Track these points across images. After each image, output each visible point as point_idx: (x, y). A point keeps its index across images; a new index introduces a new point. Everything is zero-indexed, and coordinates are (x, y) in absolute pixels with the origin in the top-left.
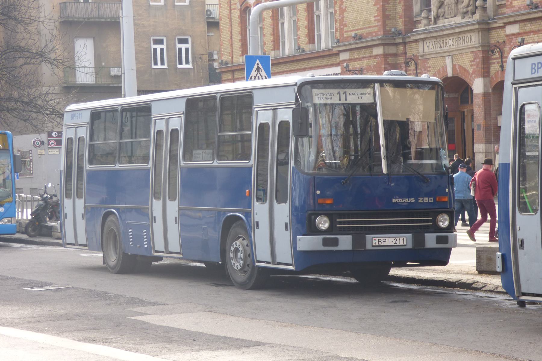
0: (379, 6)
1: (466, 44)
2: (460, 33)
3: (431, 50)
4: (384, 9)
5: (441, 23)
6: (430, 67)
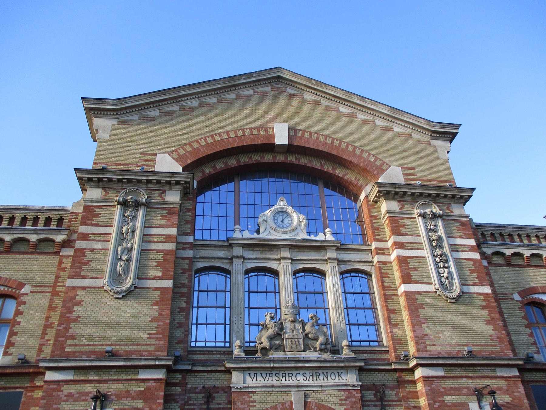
2: (320, 368)
6: (255, 402)
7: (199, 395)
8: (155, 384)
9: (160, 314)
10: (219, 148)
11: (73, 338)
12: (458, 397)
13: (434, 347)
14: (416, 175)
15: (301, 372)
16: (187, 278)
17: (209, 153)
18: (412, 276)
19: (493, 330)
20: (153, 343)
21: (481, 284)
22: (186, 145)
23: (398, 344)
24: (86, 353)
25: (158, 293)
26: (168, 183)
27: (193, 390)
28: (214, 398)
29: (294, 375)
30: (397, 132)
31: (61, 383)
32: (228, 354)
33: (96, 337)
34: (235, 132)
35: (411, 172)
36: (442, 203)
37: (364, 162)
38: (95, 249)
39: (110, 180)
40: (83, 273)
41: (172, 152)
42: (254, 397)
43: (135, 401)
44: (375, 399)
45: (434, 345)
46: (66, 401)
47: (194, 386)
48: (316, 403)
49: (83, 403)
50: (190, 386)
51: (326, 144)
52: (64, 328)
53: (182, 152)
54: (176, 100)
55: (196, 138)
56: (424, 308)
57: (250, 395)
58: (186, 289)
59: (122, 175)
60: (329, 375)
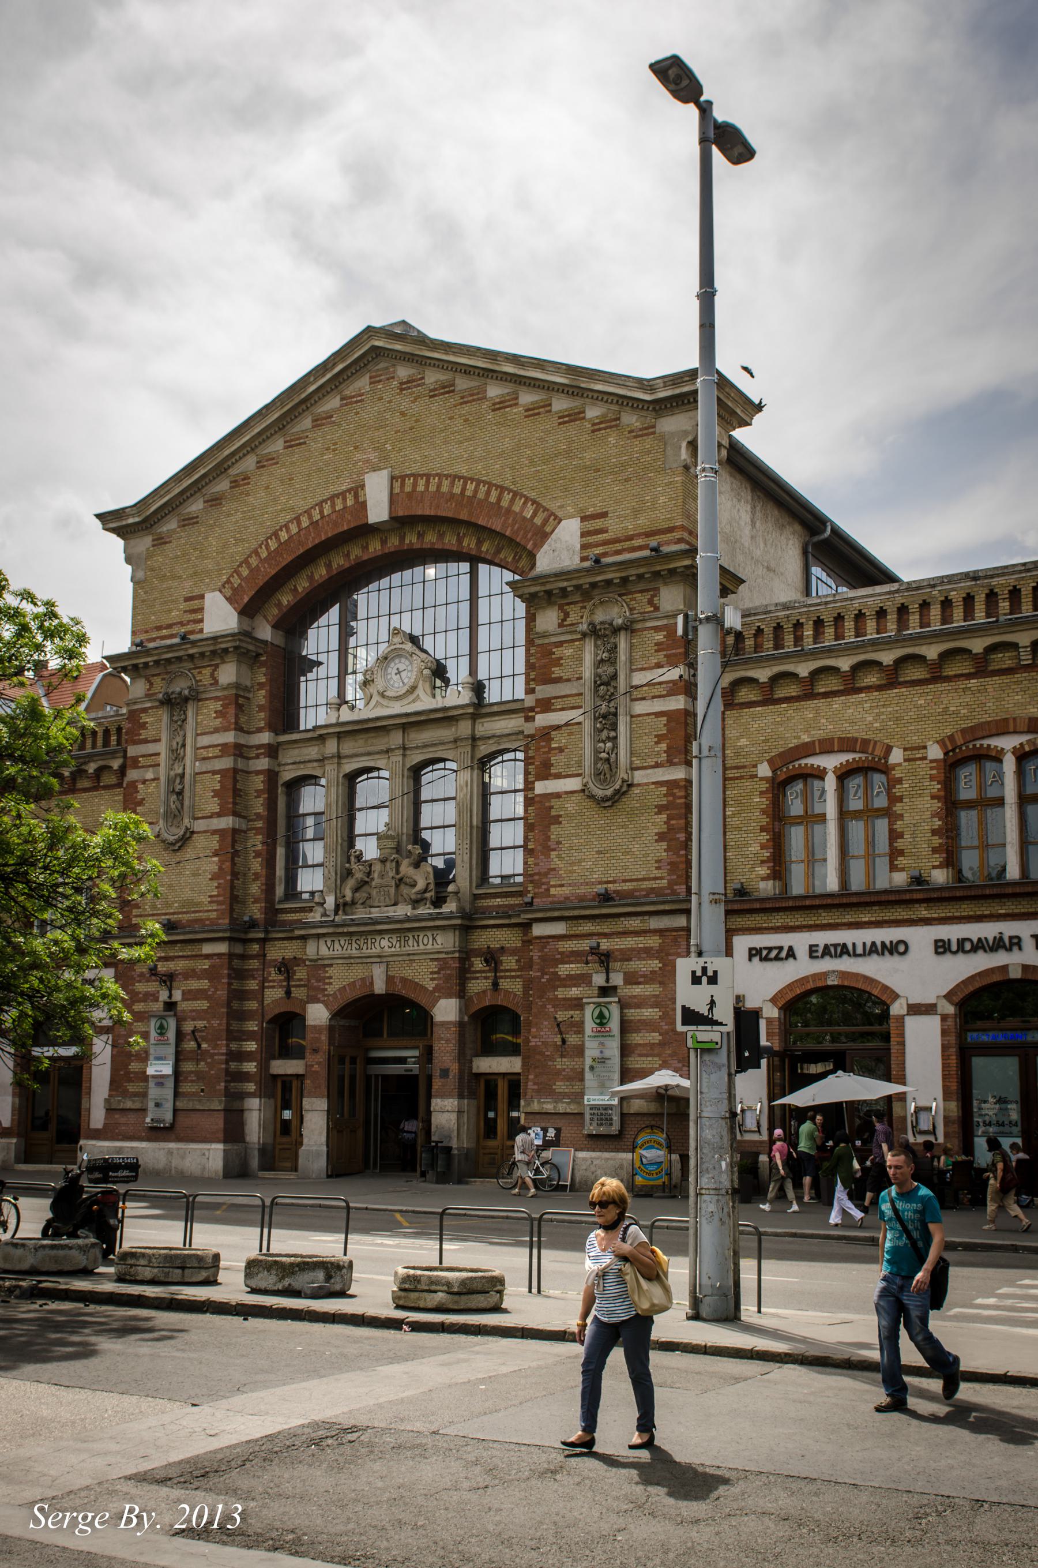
0: (222, 881)
1: (422, 947)
3: (336, 952)
4: (232, 887)
5: (361, 914)
6: (331, 978)
9: (220, 868)
10: (287, 559)
14: (607, 532)
15: (387, 937)
17: (273, 572)
18: (552, 765)
19: (665, 850)
21: (670, 763)
25: (217, 837)
28: (294, 972)
34: (308, 512)
35: (598, 524)
42: (331, 971)
45: (562, 886)
46: (139, 982)
48: (401, 978)
51: (452, 495)
53: (236, 581)
54: (221, 469)
55: (254, 545)
59: (157, 654)
60: (421, 938)
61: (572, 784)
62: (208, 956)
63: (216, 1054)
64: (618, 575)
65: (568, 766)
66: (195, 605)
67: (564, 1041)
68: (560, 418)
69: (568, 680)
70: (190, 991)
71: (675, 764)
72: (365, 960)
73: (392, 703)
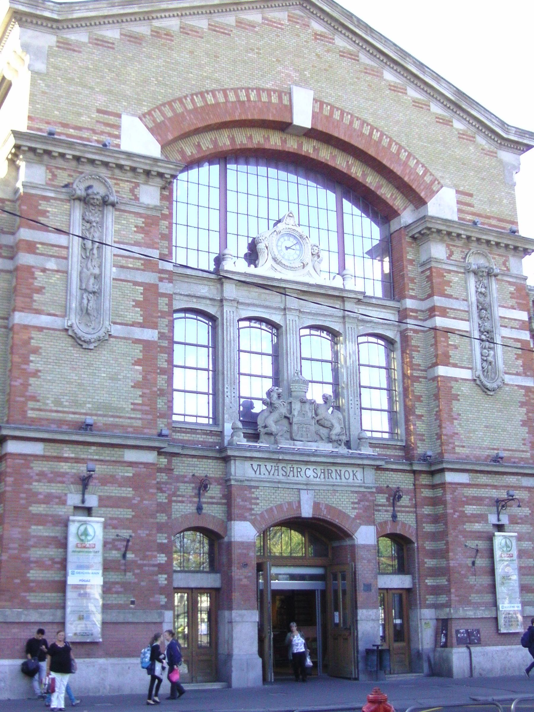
0: (147, 391)
1: (344, 480)
3: (263, 476)
6: (258, 499)
7: (188, 485)
8: (145, 469)
9: (144, 378)
11: (34, 398)
12: (479, 507)
13: (461, 449)
14: (473, 207)
15: (312, 468)
16: (167, 326)
18: (450, 356)
19: (527, 433)
20: (139, 416)
22: (164, 105)
23: (420, 440)
24: (53, 421)
25: (140, 347)
26: (147, 173)
27: (181, 479)
29: (303, 471)
30: (457, 130)
31: (29, 458)
32: (218, 435)
33: (65, 400)
34: (235, 90)
35: (467, 199)
36: (499, 255)
37: (410, 174)
38: (49, 270)
39: (62, 156)
40: (35, 306)
41: (144, 115)
42: (257, 493)
43: (123, 489)
44: (387, 503)
45: (463, 447)
46: (39, 481)
47: (182, 474)
48: (326, 505)
49: (59, 485)
50: (177, 473)
51: (362, 135)
52: (21, 384)
53: (159, 119)
55: (178, 94)
56: (458, 400)
57: (253, 490)
58: (167, 342)
59: (80, 151)
61: (466, 374)
62: (131, 464)
63: (145, 565)
64: (496, 240)
65: (462, 360)
66: (111, 122)
67: (473, 563)
68: (437, 118)
69: (457, 299)
70: (109, 498)
71: (527, 376)
72: (291, 486)
73: (284, 271)
